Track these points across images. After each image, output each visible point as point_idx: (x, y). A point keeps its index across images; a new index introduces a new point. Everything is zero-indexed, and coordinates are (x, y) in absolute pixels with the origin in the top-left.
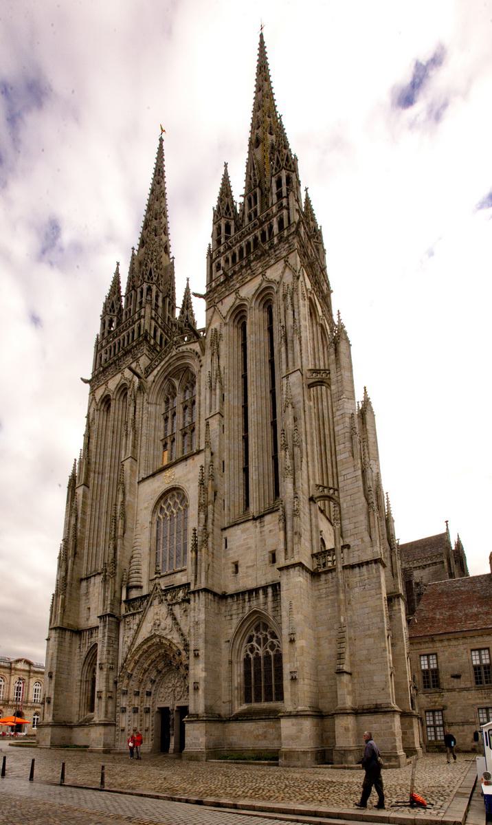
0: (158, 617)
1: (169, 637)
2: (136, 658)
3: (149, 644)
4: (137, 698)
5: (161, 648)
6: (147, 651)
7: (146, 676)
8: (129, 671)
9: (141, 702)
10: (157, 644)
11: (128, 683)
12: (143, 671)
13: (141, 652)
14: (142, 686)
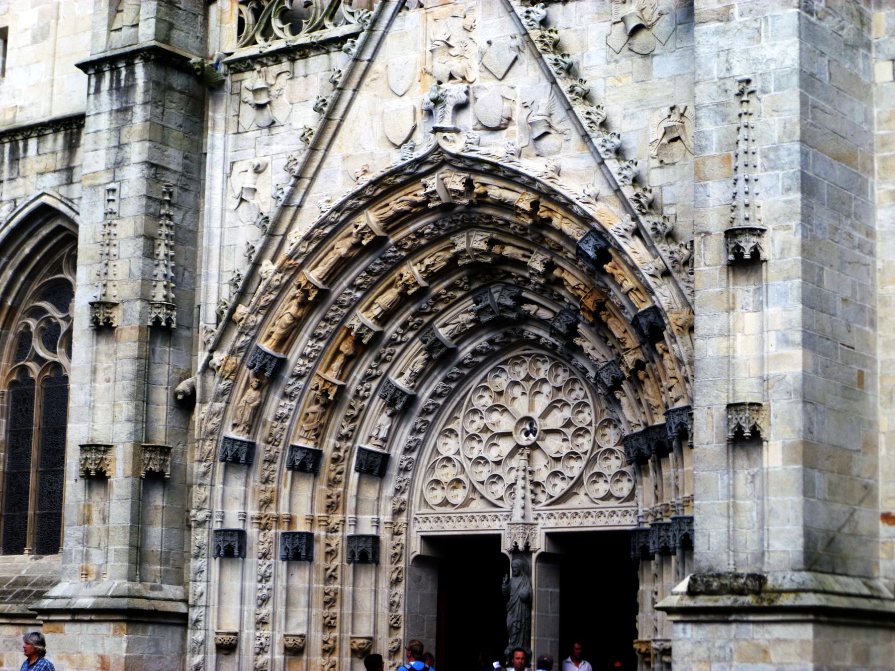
0: (456, 66)
1: (531, 167)
2: (314, 275)
3: (396, 204)
4: (304, 488)
5: (468, 225)
6: (379, 243)
7: (358, 374)
8: (267, 346)
9: (331, 507)
10: (447, 208)
11: (258, 411)
12: (346, 348)
13: (341, 246)
14: (338, 423)
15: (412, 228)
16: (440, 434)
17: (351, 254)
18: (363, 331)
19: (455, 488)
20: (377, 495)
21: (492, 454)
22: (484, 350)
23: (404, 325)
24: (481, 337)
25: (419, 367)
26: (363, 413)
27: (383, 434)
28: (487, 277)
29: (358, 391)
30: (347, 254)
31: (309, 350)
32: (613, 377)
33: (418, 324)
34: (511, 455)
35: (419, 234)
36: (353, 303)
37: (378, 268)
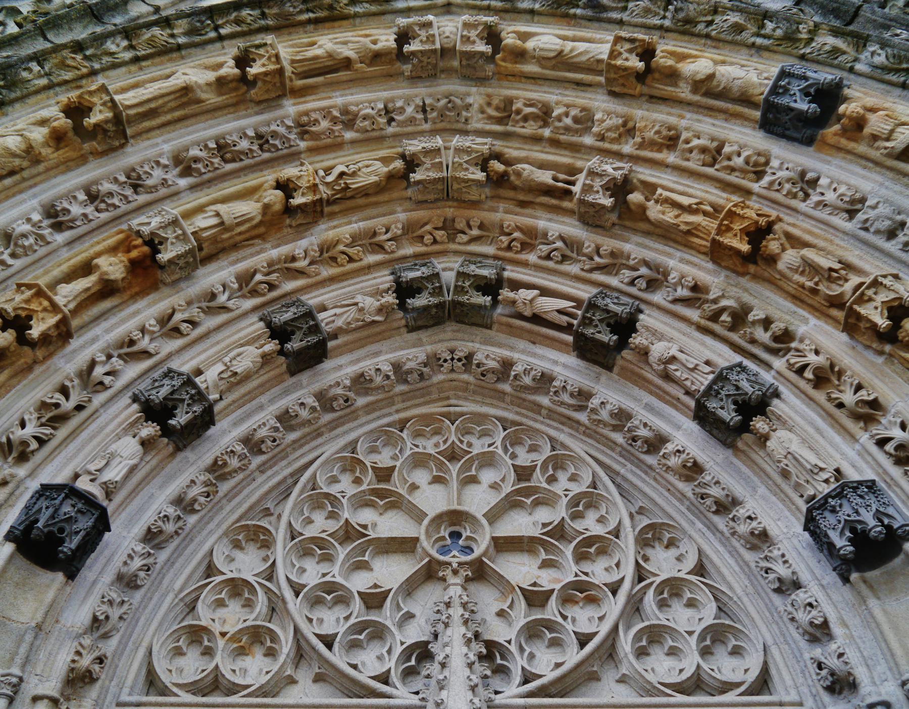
15: (339, 99)
16: (226, 534)
17: (204, 96)
18: (170, 234)
19: (242, 652)
20: (39, 617)
21: (359, 582)
22: (378, 379)
23: (245, 279)
24: (377, 354)
25: (242, 365)
26: (84, 414)
27: (114, 474)
28: (440, 234)
29: (93, 364)
30: (199, 86)
31: (27, 227)
32: (735, 403)
33: (272, 287)
34: (410, 587)
35: (349, 119)
36: (163, 191)
37: (244, 144)
